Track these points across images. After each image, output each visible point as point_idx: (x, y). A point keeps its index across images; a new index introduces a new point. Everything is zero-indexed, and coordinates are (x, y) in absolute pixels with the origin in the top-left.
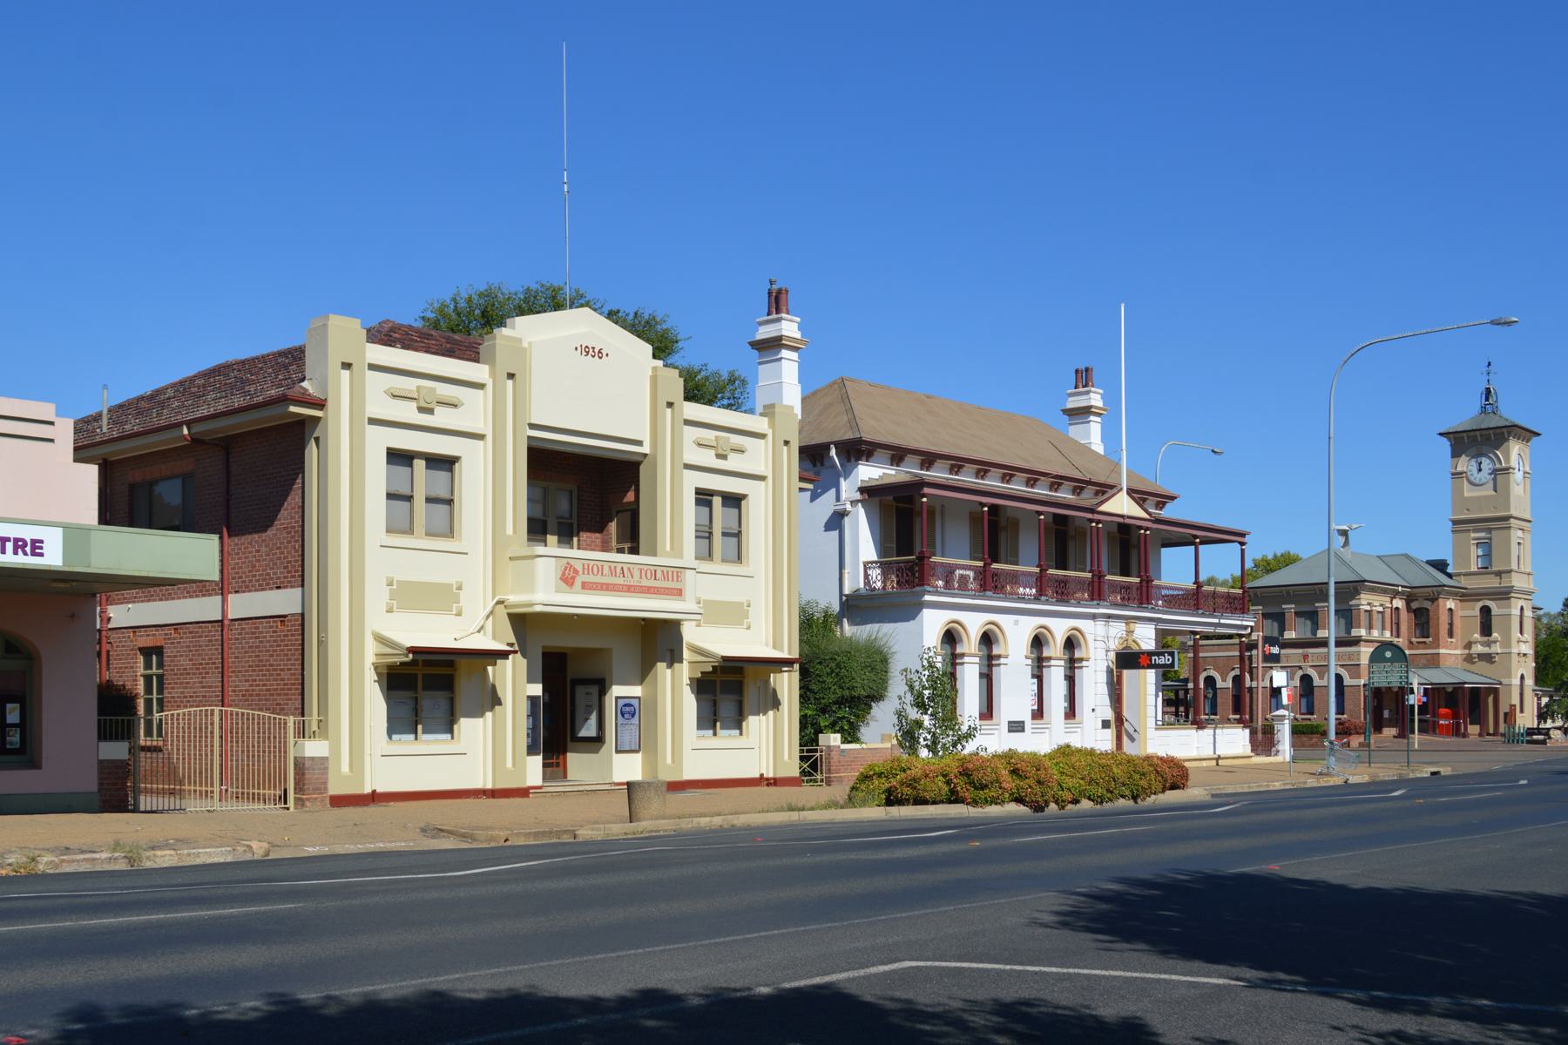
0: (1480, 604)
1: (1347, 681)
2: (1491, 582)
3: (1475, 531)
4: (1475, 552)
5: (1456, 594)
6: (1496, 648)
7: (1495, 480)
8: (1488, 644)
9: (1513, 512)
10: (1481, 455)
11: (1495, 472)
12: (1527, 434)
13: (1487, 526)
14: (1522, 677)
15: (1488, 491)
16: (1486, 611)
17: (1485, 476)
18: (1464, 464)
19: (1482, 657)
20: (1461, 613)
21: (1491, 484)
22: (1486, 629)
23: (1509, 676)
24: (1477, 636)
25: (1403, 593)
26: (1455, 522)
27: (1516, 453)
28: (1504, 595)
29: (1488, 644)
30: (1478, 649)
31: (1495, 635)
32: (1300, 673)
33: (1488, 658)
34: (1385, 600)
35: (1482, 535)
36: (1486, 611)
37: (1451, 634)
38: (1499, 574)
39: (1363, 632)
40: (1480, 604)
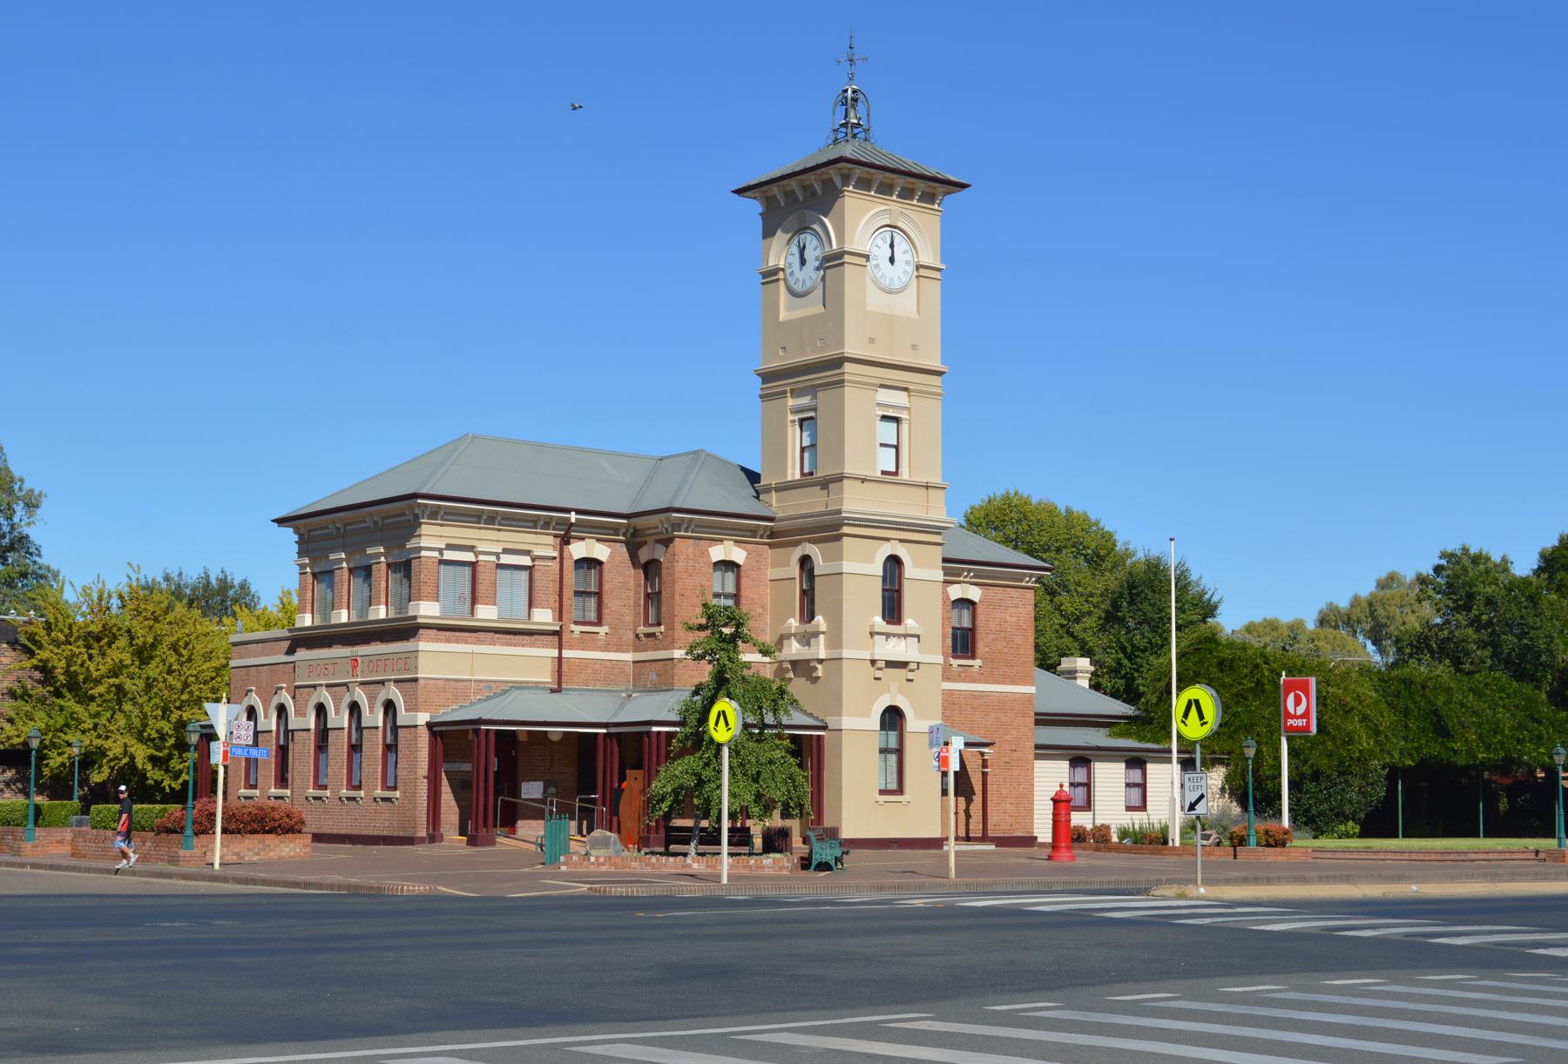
1: (403, 717)
2: (811, 503)
3: (796, 393)
4: (795, 438)
5: (754, 532)
6: (821, 650)
8: (806, 639)
9: (850, 350)
10: (804, 229)
12: (926, 187)
13: (808, 379)
17: (808, 276)
18: (780, 253)
21: (818, 293)
24: (794, 623)
25: (615, 529)
26: (767, 377)
27: (863, 220)
28: (830, 529)
29: (806, 639)
31: (819, 619)
32: (347, 699)
34: (543, 545)
35: (805, 401)
38: (825, 484)
39: (427, 610)
40: (798, 552)
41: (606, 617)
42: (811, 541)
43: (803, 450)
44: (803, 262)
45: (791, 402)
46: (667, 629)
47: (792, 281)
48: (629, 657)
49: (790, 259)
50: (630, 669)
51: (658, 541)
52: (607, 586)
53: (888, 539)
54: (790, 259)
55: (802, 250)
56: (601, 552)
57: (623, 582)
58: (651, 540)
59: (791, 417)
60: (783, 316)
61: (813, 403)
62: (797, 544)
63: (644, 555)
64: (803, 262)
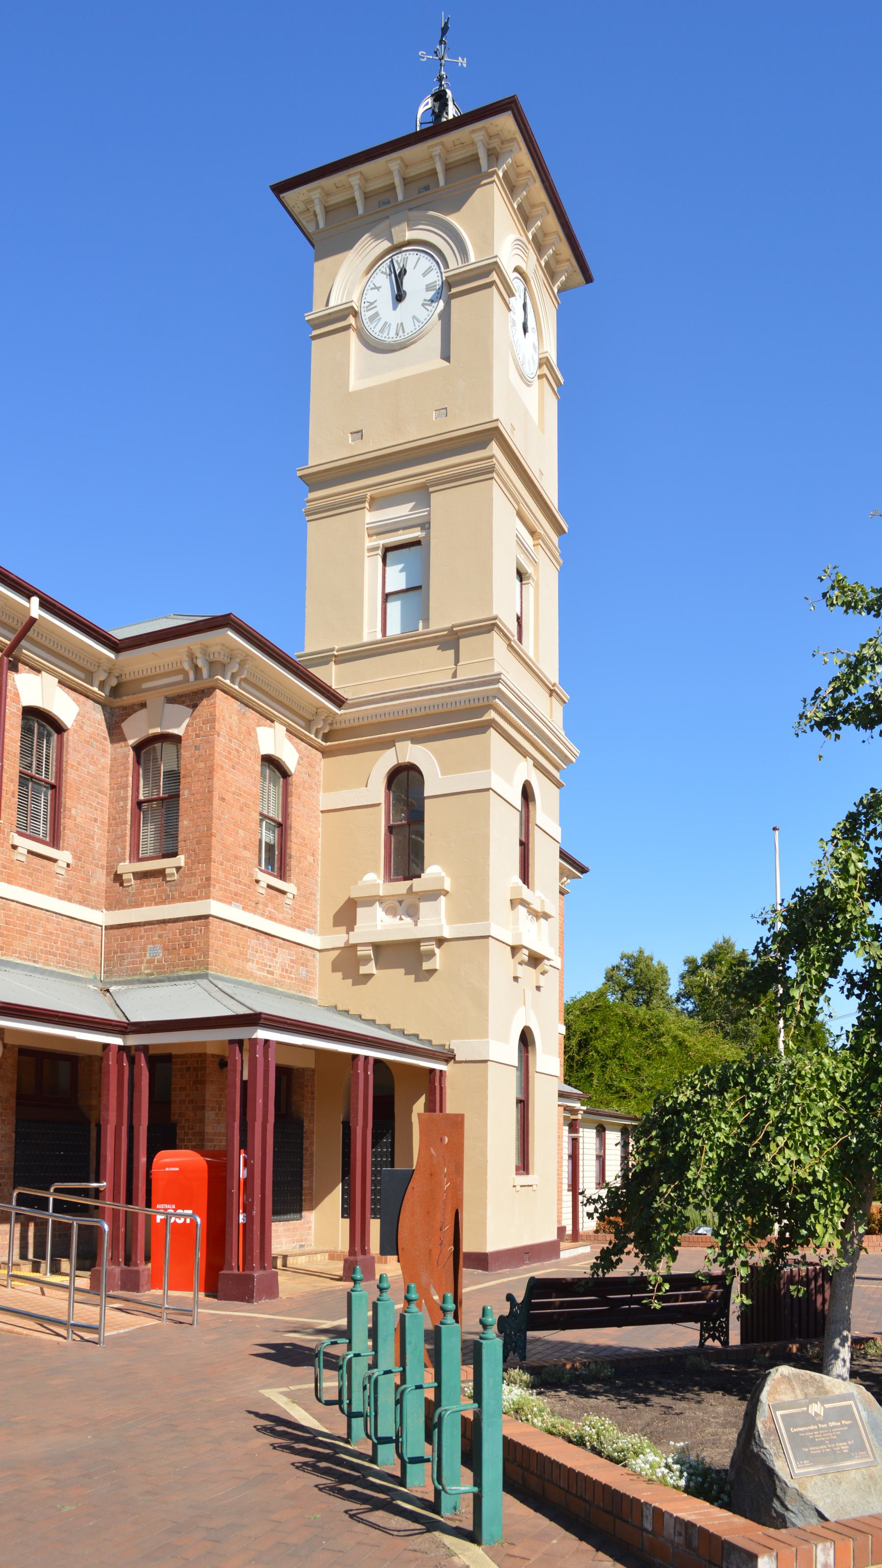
0: (387, 760)
2: (429, 670)
3: (377, 503)
6: (435, 920)
7: (445, 317)
8: (408, 907)
11: (449, 290)
14: (526, 1039)
15: (425, 358)
16: (405, 782)
17: (418, 312)
19: (391, 953)
20: (326, 800)
22: (406, 852)
23: (482, 1032)
24: (375, 880)
29: (408, 907)
30: (378, 925)
33: (407, 956)
35: (402, 511)
36: (405, 782)
37: (277, 859)
41: (68, 835)
42: (416, 739)
43: (386, 597)
44: (399, 297)
45: (371, 517)
46: (193, 861)
47: (374, 330)
48: (101, 917)
49: (371, 296)
50: (98, 939)
51: (171, 700)
52: (71, 776)
53: (525, 754)
54: (371, 296)
55: (399, 277)
56: (65, 707)
57: (94, 764)
58: (155, 701)
59: (369, 543)
60: (354, 384)
61: (422, 513)
62: (389, 744)
63: (137, 728)
64: (399, 297)
